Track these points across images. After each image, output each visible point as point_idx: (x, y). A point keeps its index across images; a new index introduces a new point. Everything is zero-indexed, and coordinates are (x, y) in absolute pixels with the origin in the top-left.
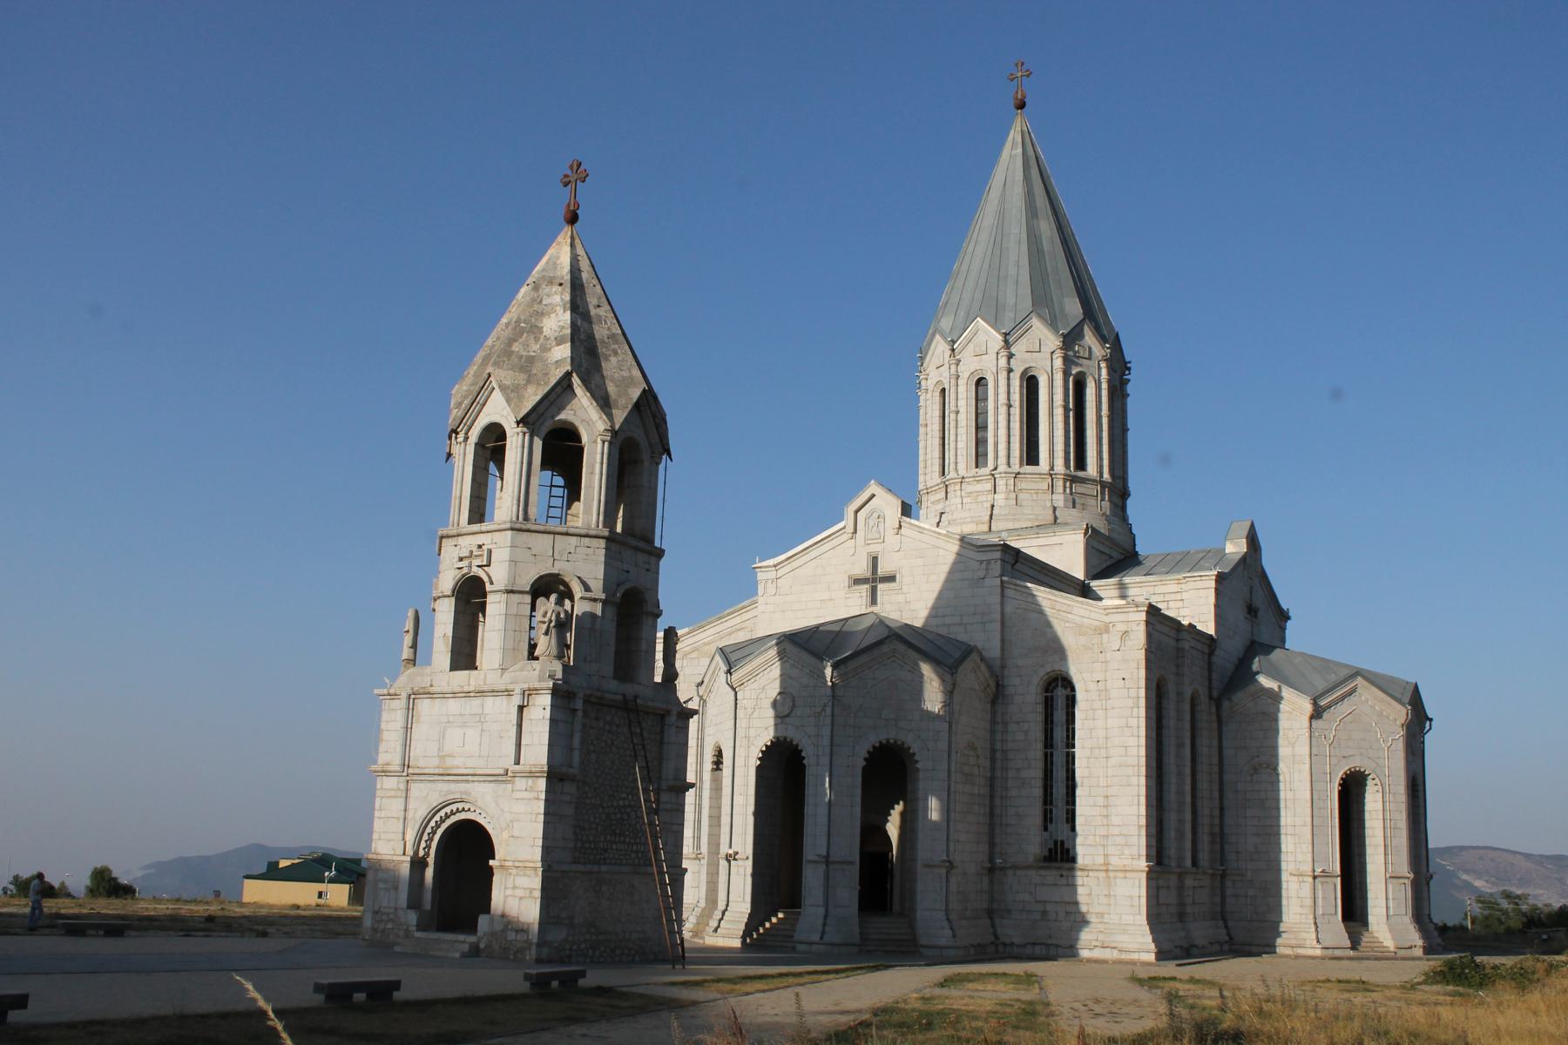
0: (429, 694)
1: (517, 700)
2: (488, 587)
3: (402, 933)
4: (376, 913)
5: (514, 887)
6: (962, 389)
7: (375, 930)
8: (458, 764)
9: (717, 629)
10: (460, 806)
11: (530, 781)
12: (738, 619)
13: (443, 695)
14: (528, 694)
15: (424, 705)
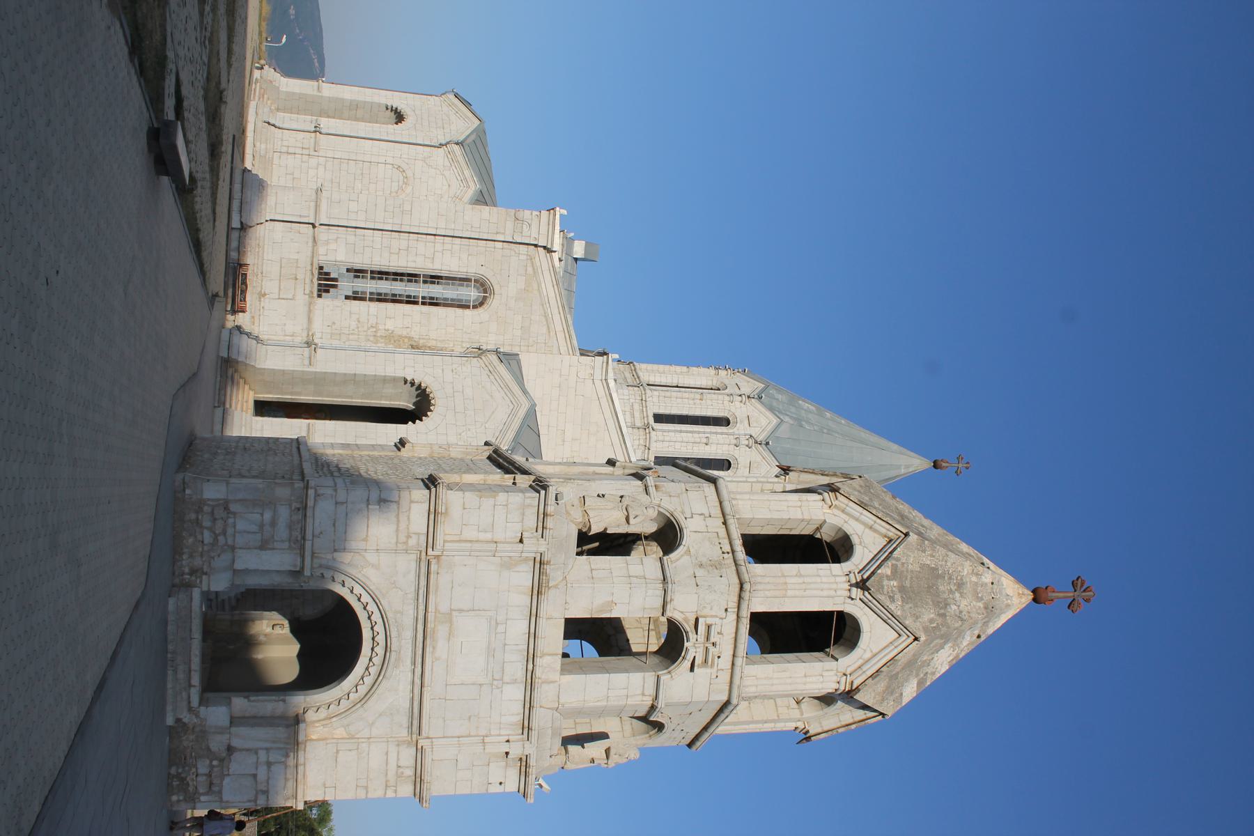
0: (538, 590)
1: (516, 750)
2: (665, 678)
3: (198, 562)
4: (226, 509)
5: (269, 764)
6: (725, 448)
7: (201, 504)
8: (440, 648)
9: (553, 301)
10: (380, 638)
11: (410, 772)
12: (559, 328)
13: (534, 615)
14: (524, 764)
15: (523, 577)
